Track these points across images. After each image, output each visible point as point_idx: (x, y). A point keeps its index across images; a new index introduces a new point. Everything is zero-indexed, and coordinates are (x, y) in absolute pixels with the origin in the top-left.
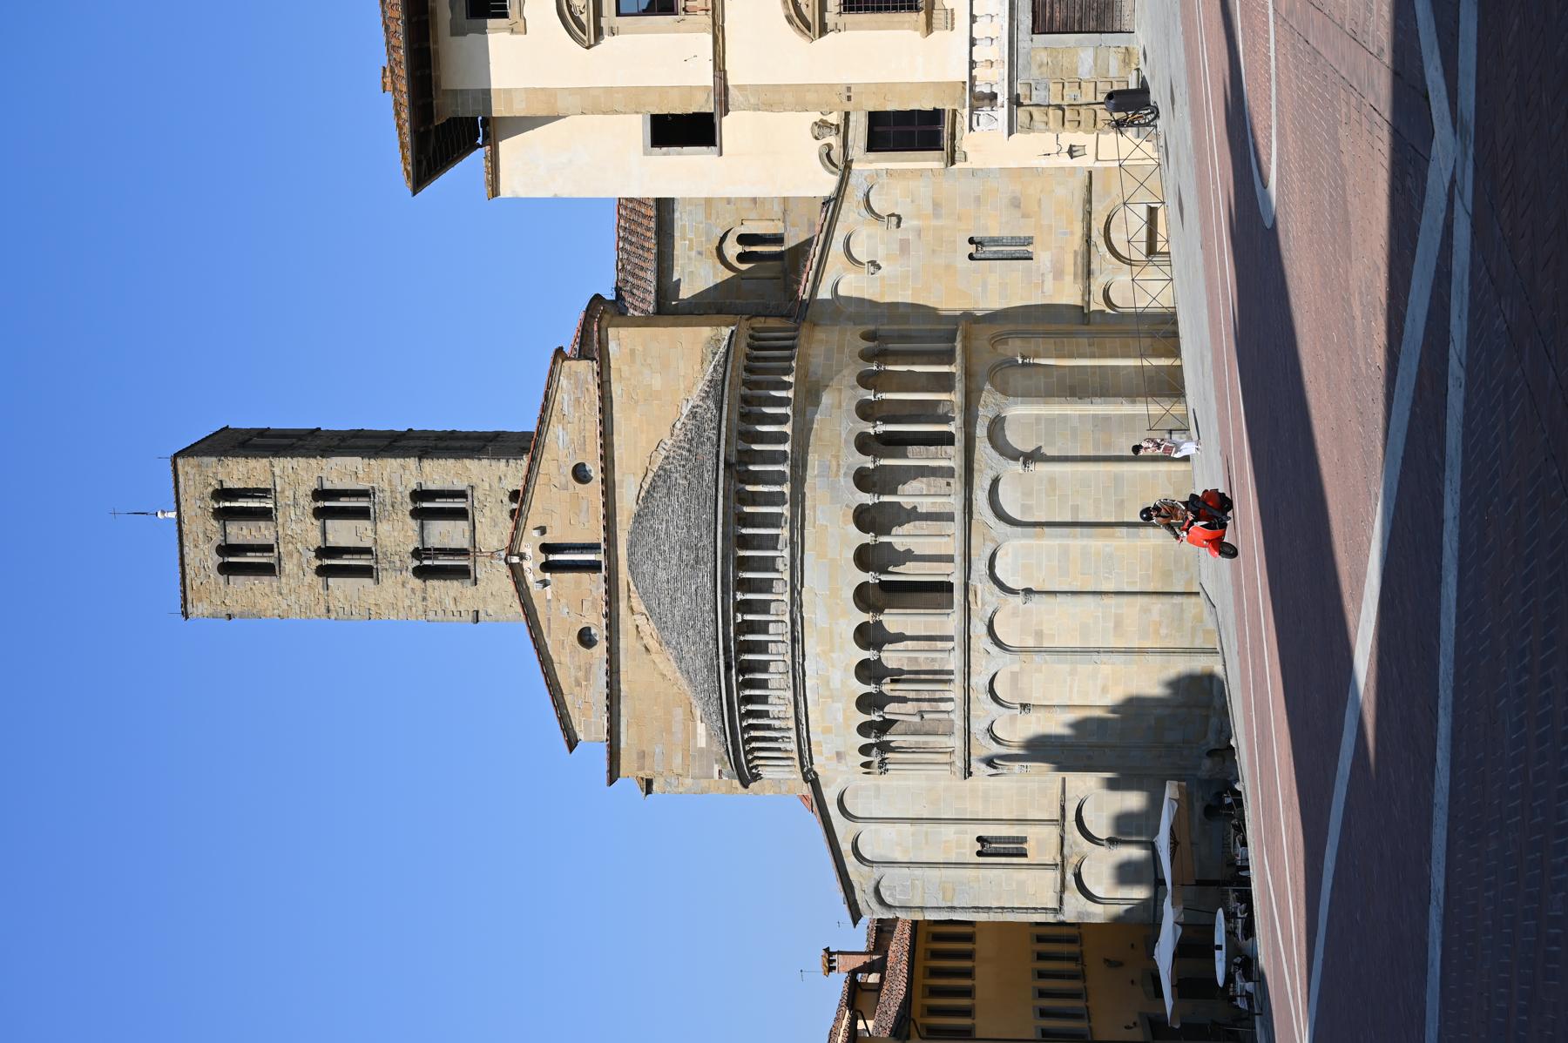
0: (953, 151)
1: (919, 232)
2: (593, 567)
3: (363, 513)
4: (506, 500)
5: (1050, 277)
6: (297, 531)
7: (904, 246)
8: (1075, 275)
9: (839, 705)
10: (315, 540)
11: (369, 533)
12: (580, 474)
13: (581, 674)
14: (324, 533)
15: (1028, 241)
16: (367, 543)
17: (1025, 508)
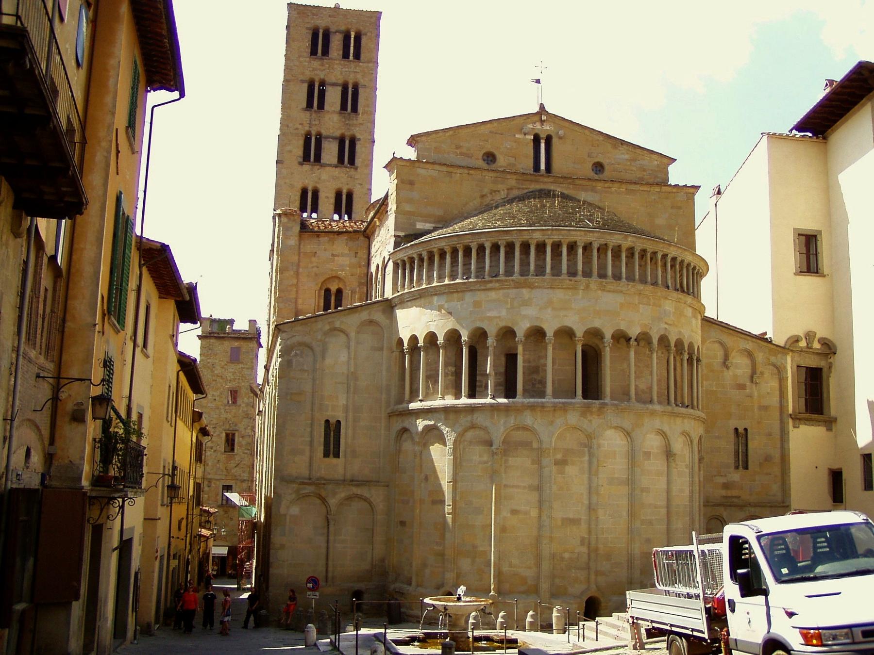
0: (800, 419)
1: (751, 396)
2: (537, 167)
3: (344, 107)
4: (349, 187)
5: (725, 481)
6: (336, 70)
7: (742, 387)
8: (726, 497)
9: (504, 313)
10: (331, 78)
11: (333, 109)
12: (599, 167)
13: (464, 150)
14: (334, 85)
15: (746, 467)
16: (326, 107)
17: (647, 454)
